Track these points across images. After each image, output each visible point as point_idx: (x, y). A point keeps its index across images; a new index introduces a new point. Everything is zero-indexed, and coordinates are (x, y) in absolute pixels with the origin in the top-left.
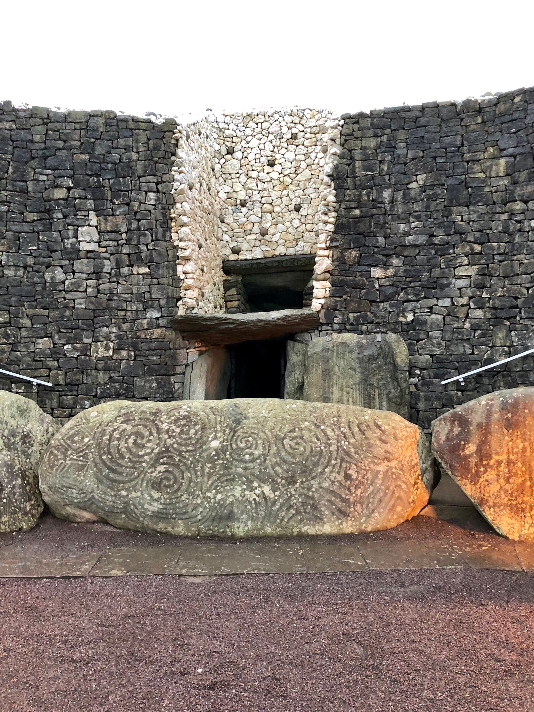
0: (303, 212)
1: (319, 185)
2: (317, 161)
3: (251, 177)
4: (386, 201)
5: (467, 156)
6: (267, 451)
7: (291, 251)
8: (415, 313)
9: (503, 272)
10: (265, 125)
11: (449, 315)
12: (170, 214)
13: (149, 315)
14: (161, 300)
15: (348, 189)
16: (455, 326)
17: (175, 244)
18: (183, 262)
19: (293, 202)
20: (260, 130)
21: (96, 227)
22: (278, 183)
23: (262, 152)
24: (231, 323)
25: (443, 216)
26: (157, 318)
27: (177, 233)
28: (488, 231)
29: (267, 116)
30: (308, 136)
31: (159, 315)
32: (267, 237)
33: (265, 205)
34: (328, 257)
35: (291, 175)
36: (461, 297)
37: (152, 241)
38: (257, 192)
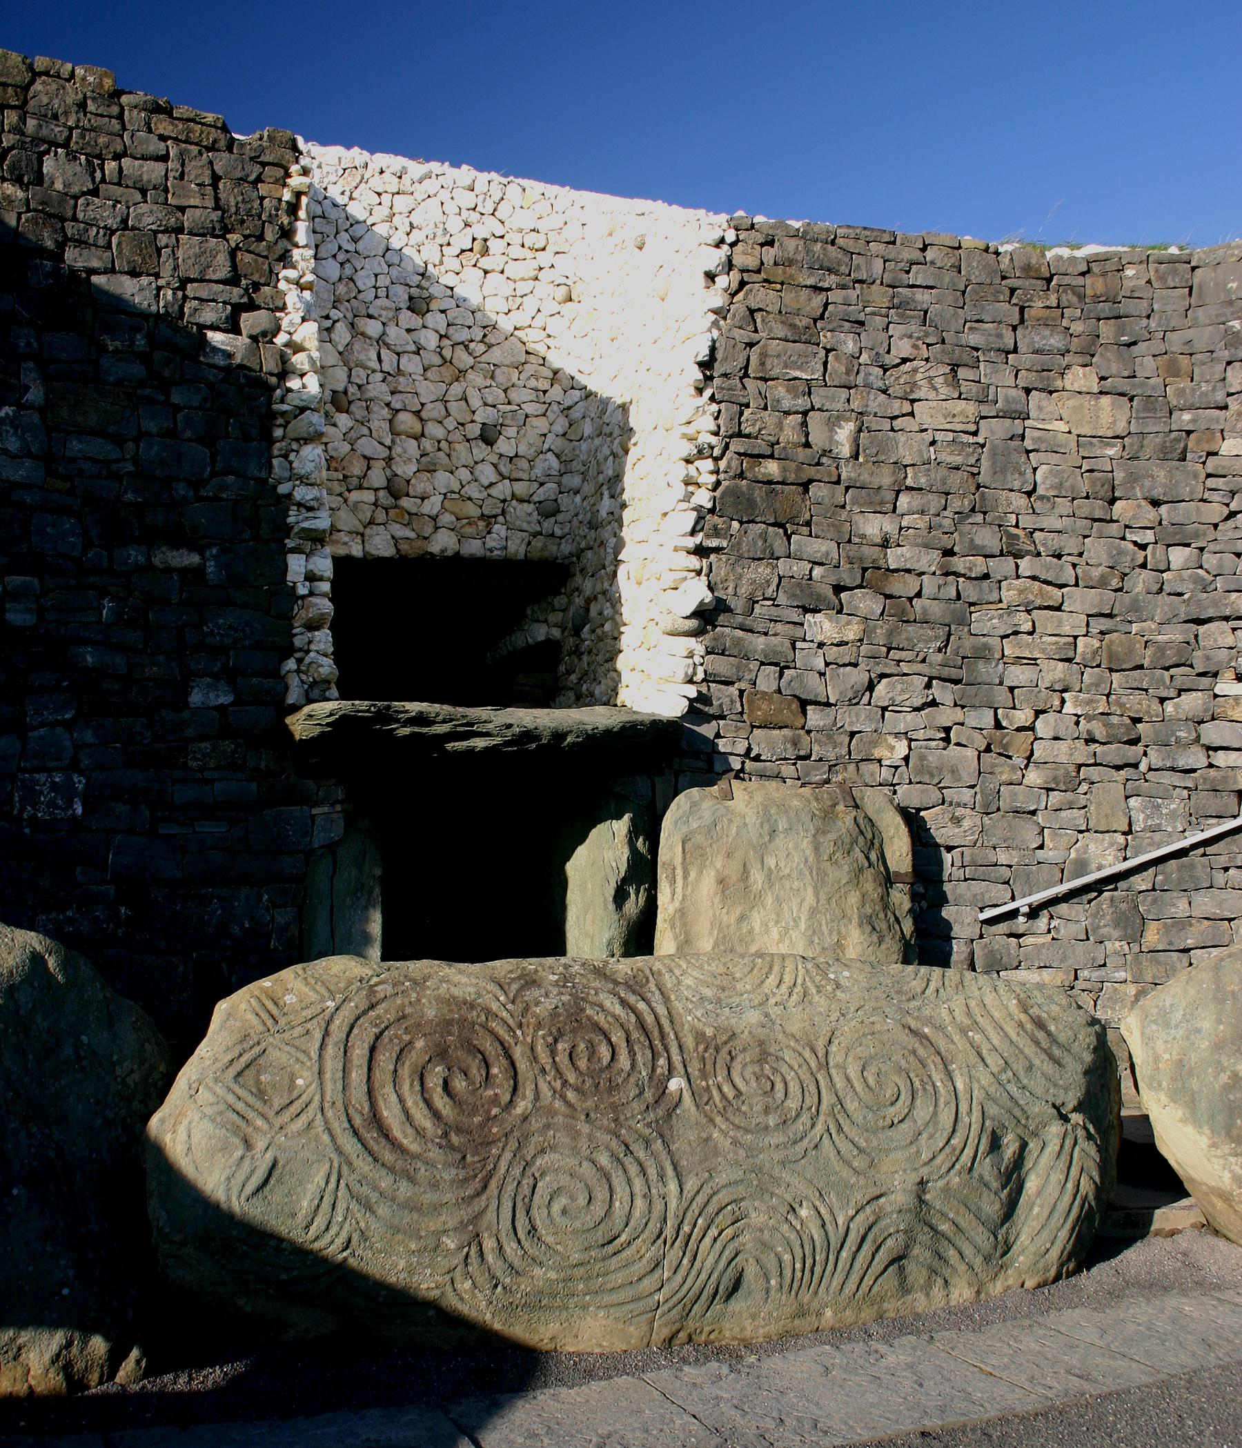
0: (503, 446)
1: (545, 385)
2: (539, 321)
3: (363, 334)
4: (846, 451)
5: (1025, 379)
6: (816, 1100)
7: (473, 548)
8: (911, 740)
9: (1112, 656)
10: (401, 203)
11: (988, 749)
12: (270, 401)
13: (196, 698)
14: (231, 653)
15: (747, 406)
16: (1004, 778)
17: (283, 489)
18: (308, 546)
19: (477, 418)
20: (387, 211)
21: (42, 410)
22: (438, 361)
23: (395, 272)
24: (487, 734)
25: (973, 510)
26: (221, 708)
27: (286, 457)
28: (1075, 560)
29: (406, 179)
30: (516, 251)
31: (225, 699)
32: (405, 503)
33: (402, 416)
34: (699, 573)
35: (472, 345)
36: (1014, 708)
37: (214, 474)
38: (379, 376)
